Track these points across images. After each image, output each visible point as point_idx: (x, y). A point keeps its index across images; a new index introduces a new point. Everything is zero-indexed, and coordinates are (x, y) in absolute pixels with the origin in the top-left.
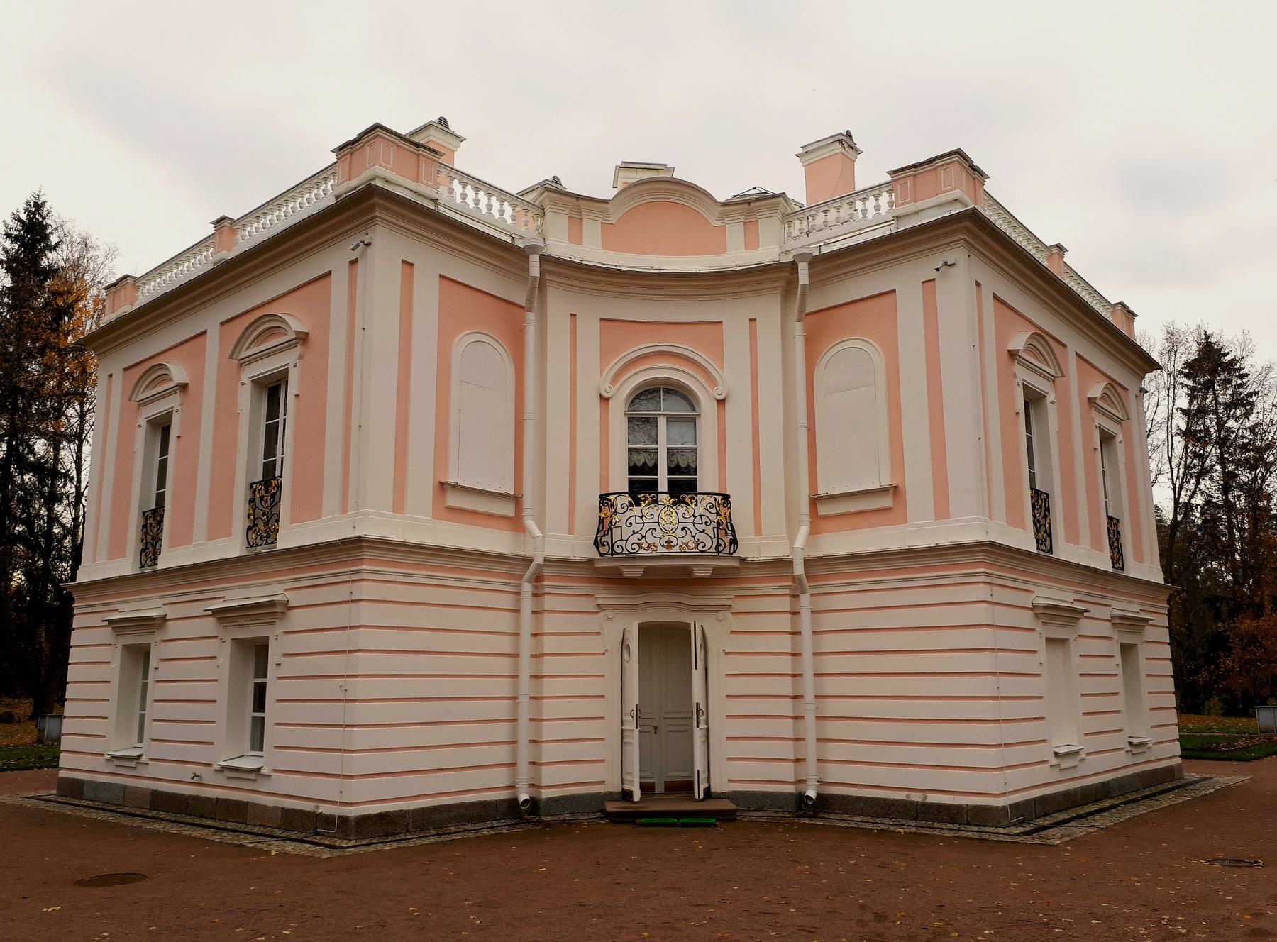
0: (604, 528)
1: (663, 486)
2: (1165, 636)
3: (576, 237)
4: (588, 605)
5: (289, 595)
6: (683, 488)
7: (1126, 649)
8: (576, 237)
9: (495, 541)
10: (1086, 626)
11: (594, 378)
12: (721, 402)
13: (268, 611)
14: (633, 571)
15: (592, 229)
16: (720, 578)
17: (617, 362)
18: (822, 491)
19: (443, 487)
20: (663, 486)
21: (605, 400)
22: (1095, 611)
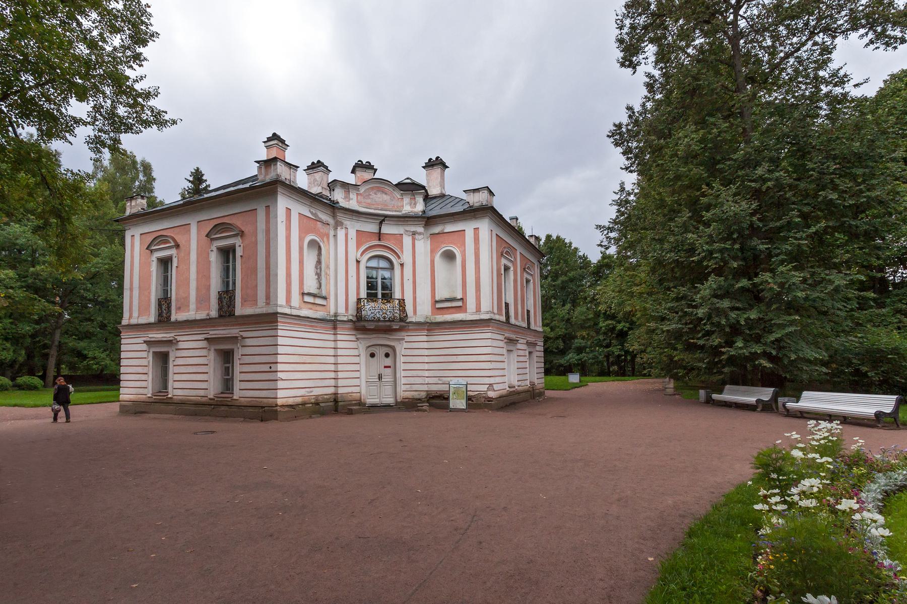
0: (359, 309)
1: (380, 296)
2: (542, 349)
3: (347, 198)
4: (353, 338)
5: (241, 333)
6: (387, 297)
7: (530, 353)
8: (347, 198)
9: (320, 314)
10: (519, 346)
11: (353, 254)
12: (402, 265)
13: (234, 339)
14: (371, 326)
15: (353, 195)
16: (401, 329)
17: (363, 248)
18: (437, 299)
19: (303, 294)
20: (380, 296)
21: (358, 262)
22: (521, 341)
